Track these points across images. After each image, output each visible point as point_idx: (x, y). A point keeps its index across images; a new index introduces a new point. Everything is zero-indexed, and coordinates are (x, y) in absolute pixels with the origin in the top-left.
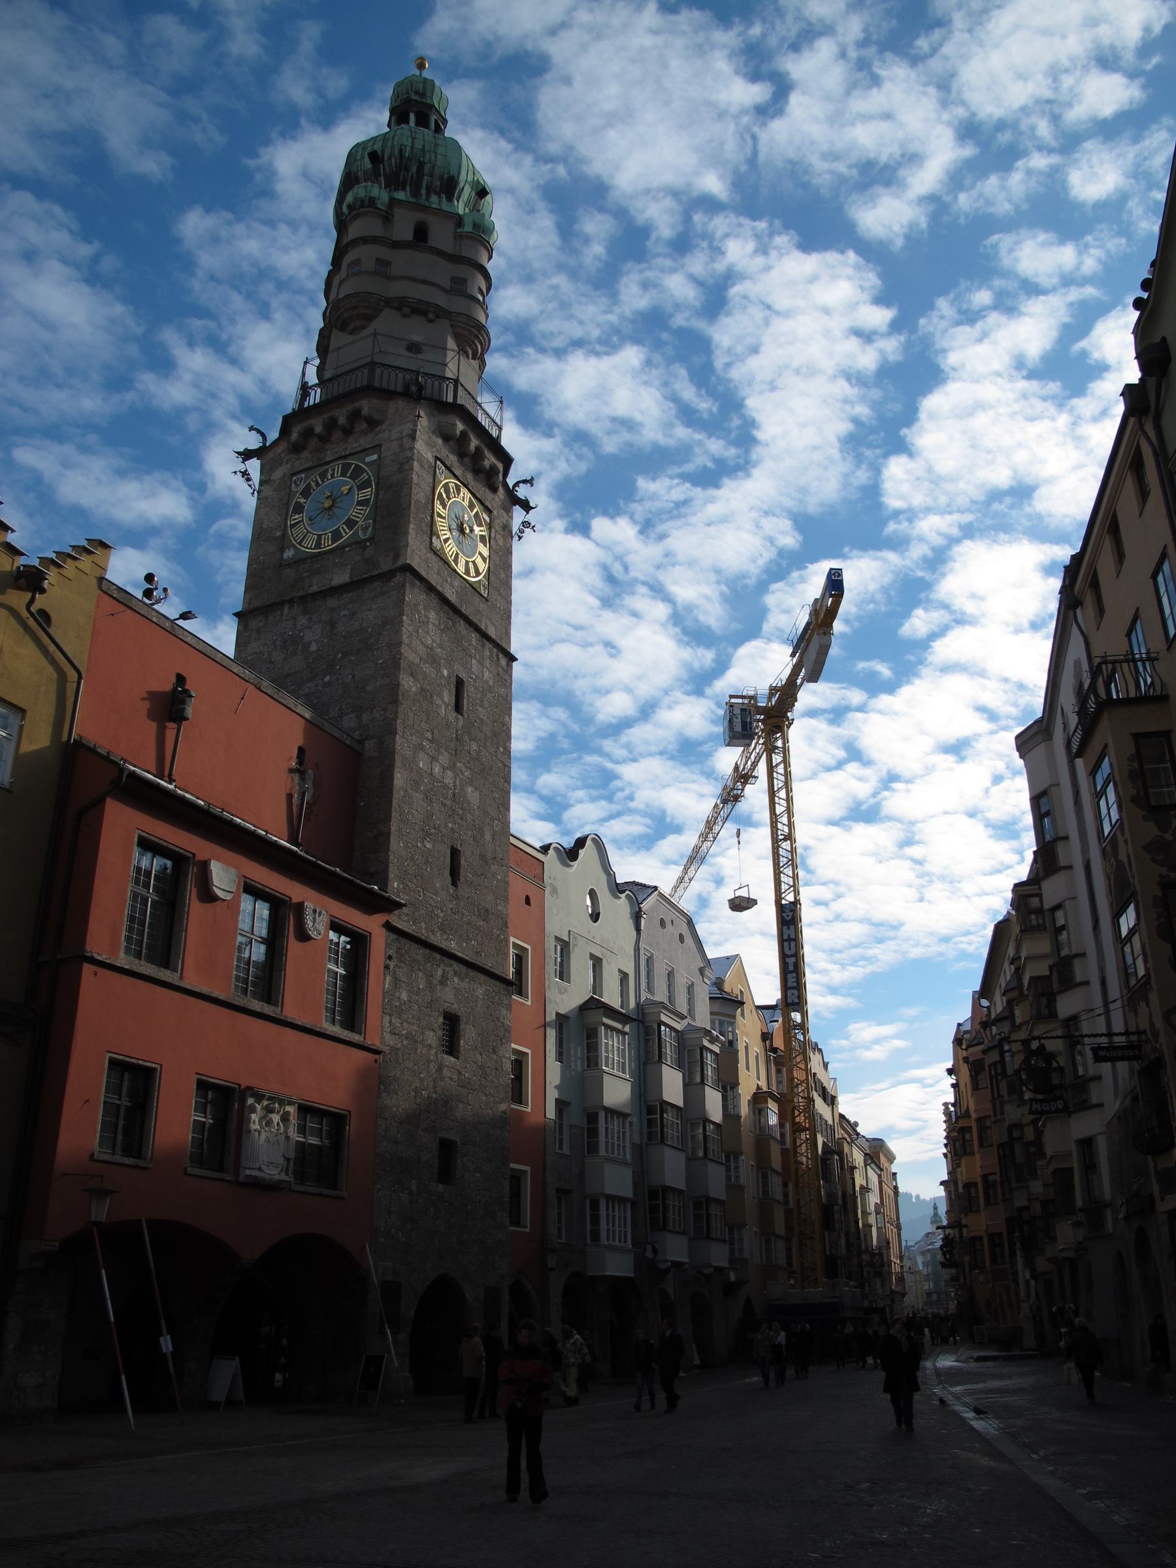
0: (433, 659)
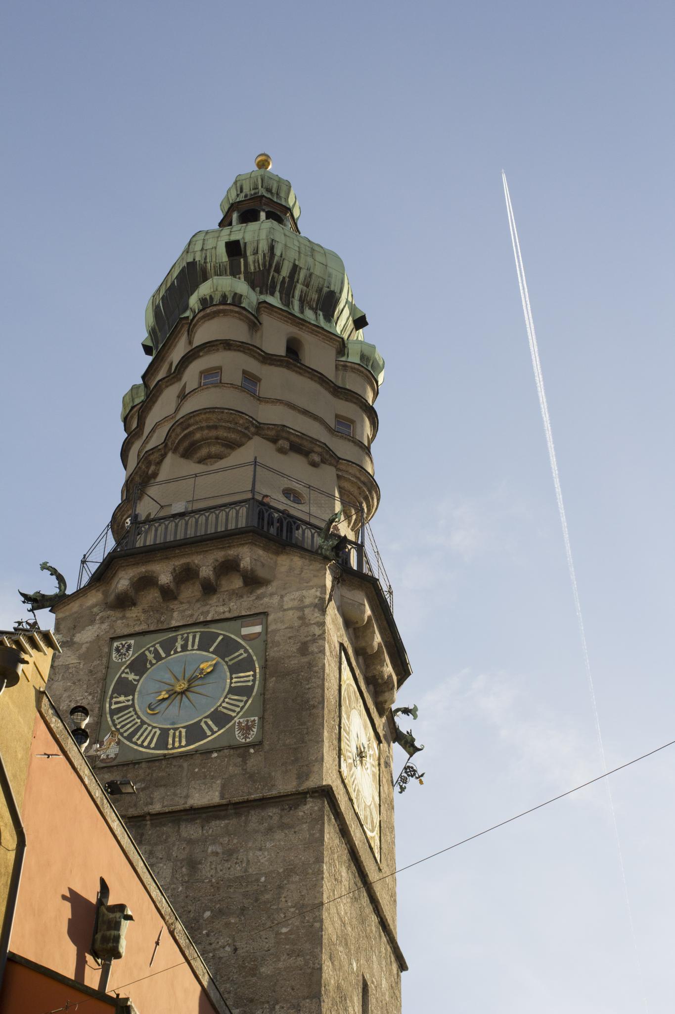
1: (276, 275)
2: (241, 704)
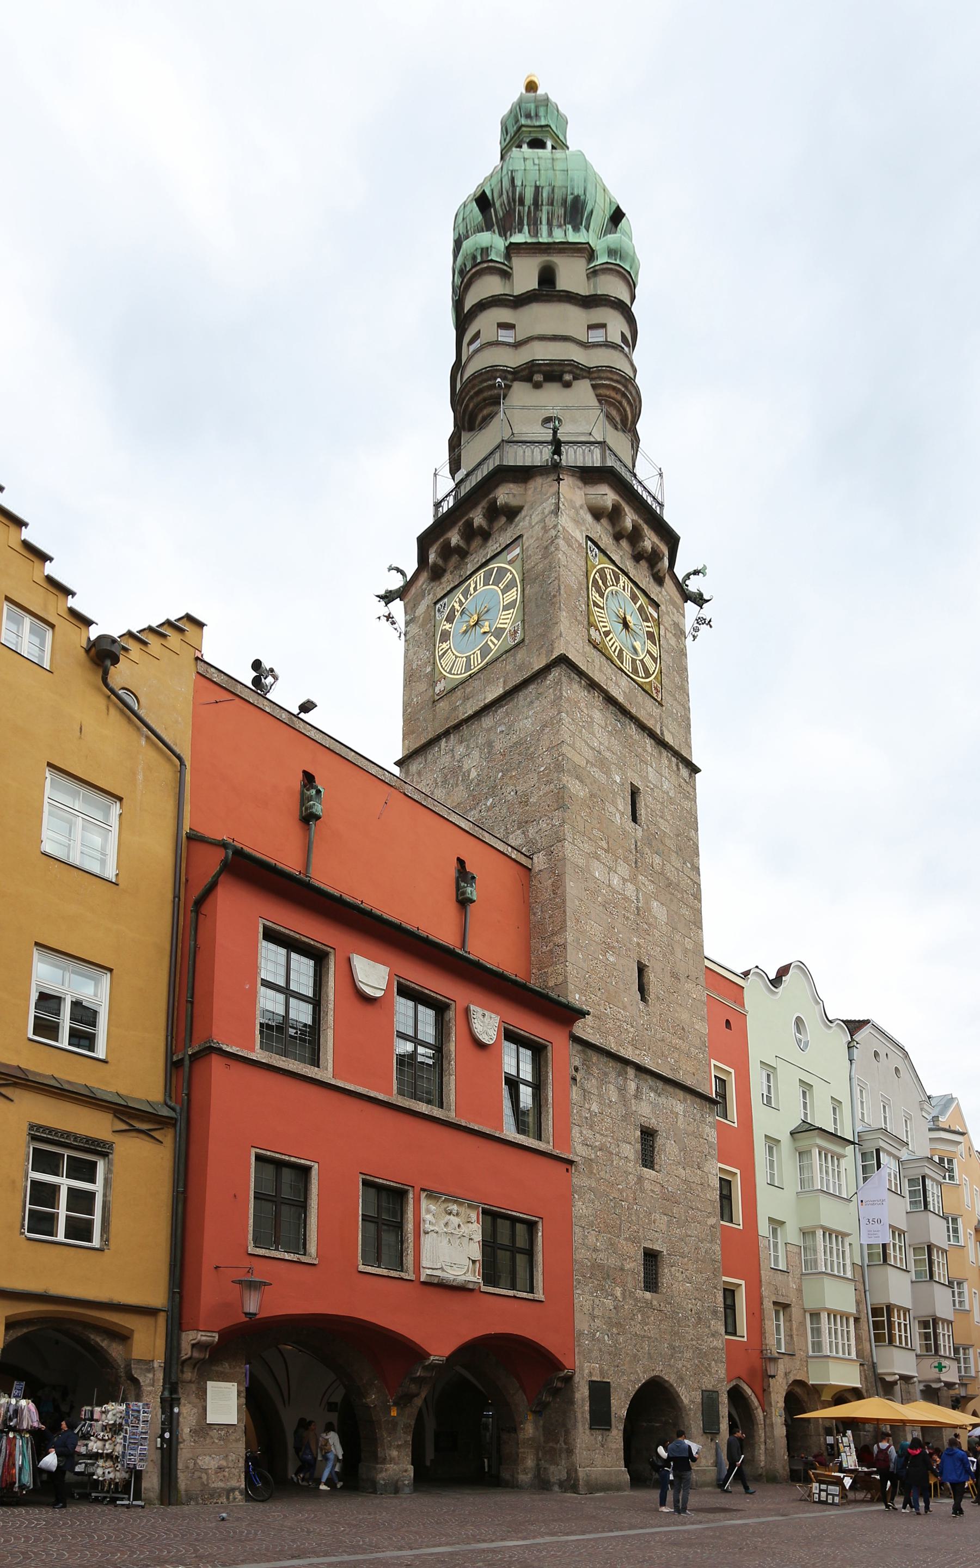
0: (602, 763)
1: (521, 208)
2: (509, 616)
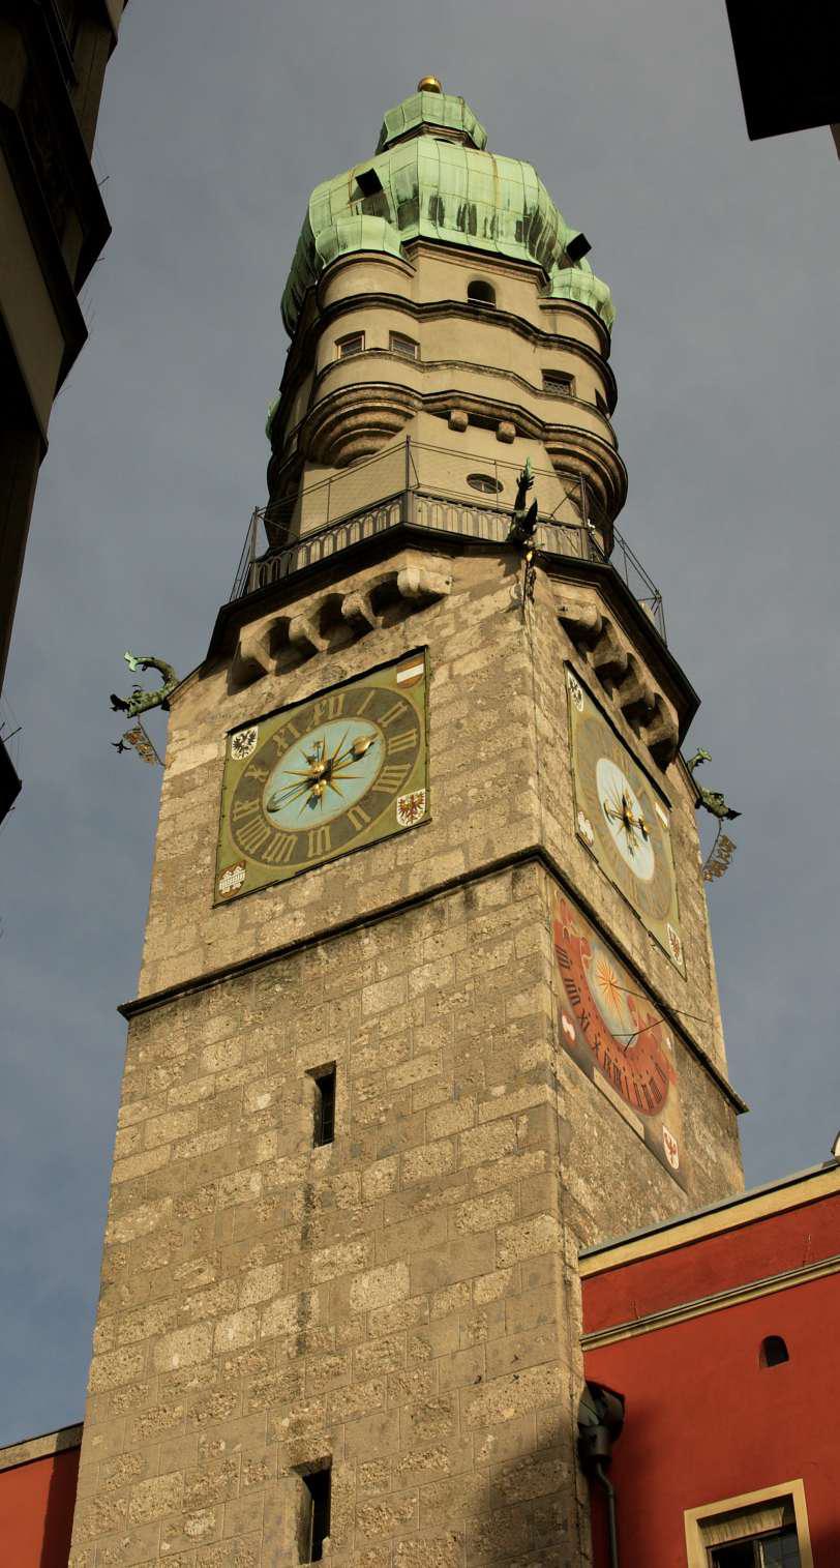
2: (403, 775)
